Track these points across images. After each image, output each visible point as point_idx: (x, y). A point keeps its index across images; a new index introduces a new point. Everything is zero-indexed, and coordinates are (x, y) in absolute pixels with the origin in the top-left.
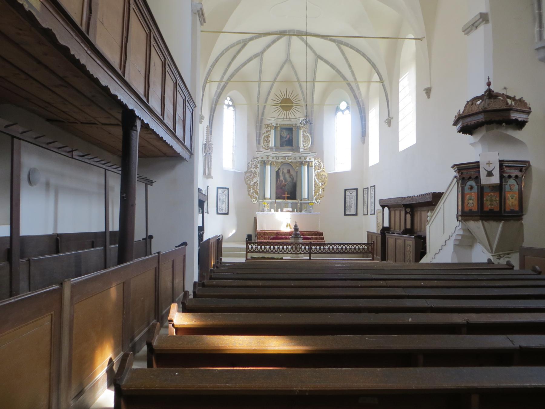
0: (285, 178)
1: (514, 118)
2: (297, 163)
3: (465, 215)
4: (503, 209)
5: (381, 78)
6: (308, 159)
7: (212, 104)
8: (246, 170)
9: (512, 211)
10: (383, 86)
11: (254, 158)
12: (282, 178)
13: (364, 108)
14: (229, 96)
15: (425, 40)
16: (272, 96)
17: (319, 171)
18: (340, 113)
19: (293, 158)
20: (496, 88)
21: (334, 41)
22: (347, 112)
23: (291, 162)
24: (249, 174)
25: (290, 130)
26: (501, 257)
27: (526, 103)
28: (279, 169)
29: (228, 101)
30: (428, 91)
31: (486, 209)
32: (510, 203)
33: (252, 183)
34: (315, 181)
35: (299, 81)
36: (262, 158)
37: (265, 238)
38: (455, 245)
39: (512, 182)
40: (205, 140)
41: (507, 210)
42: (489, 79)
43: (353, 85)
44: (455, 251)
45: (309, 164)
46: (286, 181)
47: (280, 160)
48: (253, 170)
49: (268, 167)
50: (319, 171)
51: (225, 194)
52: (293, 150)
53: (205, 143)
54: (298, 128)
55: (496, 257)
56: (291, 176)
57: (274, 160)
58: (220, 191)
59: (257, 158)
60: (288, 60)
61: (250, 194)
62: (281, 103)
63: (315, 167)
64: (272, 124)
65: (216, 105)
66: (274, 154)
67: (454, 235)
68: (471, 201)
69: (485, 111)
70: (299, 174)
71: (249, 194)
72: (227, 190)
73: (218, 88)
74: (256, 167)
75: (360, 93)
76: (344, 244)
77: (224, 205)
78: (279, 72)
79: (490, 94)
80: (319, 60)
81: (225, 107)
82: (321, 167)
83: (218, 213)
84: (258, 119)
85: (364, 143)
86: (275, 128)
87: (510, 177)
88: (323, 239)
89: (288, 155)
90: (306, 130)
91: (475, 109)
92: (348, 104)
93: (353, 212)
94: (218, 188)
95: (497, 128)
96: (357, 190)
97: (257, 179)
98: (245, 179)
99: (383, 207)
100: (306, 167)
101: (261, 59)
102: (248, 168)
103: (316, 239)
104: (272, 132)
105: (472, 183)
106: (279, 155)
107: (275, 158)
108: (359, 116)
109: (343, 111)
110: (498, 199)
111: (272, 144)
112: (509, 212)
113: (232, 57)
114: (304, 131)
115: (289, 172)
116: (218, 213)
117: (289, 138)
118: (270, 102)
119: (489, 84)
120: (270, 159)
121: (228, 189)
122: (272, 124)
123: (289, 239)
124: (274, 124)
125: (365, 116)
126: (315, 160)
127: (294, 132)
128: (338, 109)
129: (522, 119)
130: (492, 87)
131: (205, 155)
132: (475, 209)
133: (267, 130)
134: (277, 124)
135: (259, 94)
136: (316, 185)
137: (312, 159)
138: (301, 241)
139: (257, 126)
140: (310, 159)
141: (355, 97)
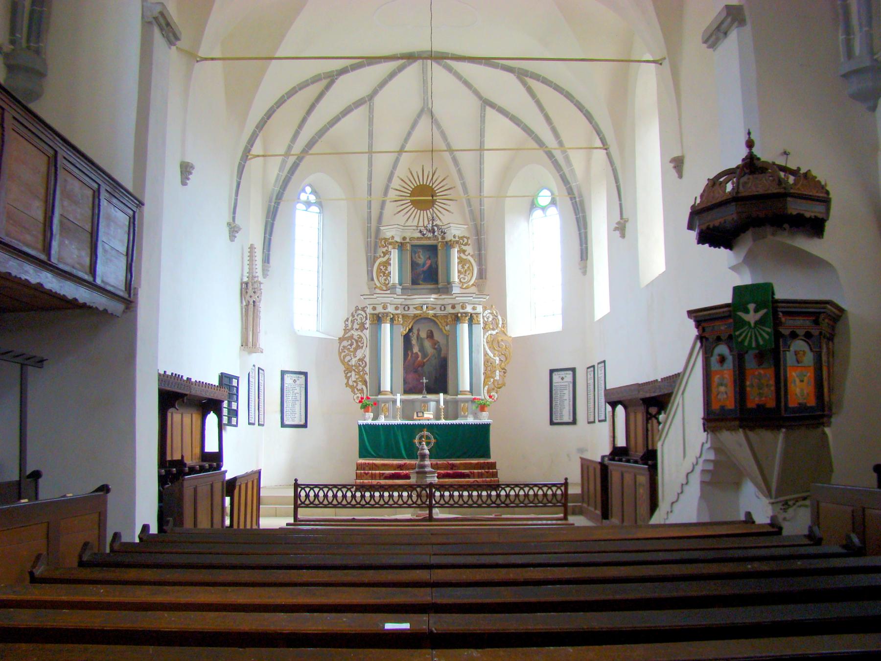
0: (423, 348)
1: (794, 213)
2: (446, 316)
3: (714, 420)
4: (783, 404)
5: (603, 140)
6: (469, 309)
7: (270, 201)
8: (341, 334)
9: (802, 408)
10: (608, 155)
11: (357, 309)
12: (416, 350)
13: (582, 203)
14: (310, 185)
15: (666, 63)
16: (396, 183)
17: (494, 332)
18: (537, 213)
19: (438, 307)
20: (765, 154)
21: (510, 70)
22: (553, 210)
23: (435, 315)
24: (348, 343)
25: (432, 250)
26: (789, 506)
27: (819, 182)
28: (410, 330)
29: (307, 195)
30: (678, 164)
31: (751, 405)
32: (798, 390)
33: (353, 362)
34: (486, 354)
35: (450, 150)
36: (374, 308)
37: (373, 477)
38: (703, 483)
39: (799, 345)
40: (246, 274)
41: (791, 405)
42: (749, 134)
43: (558, 155)
44: (703, 496)
45: (472, 319)
46: (425, 355)
47: (412, 312)
48: (356, 334)
49: (386, 327)
50: (494, 332)
51: (300, 385)
52: (438, 291)
53: (245, 279)
54: (448, 245)
55: (780, 506)
56: (435, 344)
57: (399, 312)
58: (288, 379)
59: (363, 309)
60: (426, 110)
61: (351, 383)
62: (413, 194)
63: (485, 323)
64: (393, 237)
65: (279, 204)
66: (400, 300)
67: (701, 461)
68: (722, 389)
69: (736, 199)
70: (452, 338)
71: (347, 384)
72: (303, 377)
73: (281, 169)
74: (362, 327)
75: (572, 171)
76: (531, 486)
77: (297, 407)
78: (409, 134)
79: (752, 165)
80: (488, 109)
81: (300, 206)
82: (497, 324)
83: (283, 425)
84: (369, 229)
85: (584, 273)
86: (401, 246)
87: (794, 336)
88: (495, 475)
89: (426, 301)
90: (464, 248)
91: (719, 197)
92: (552, 194)
93: (567, 418)
94: (283, 373)
95: (773, 234)
96: (573, 370)
97: (365, 352)
98: (340, 353)
99: (614, 405)
100: (465, 326)
101: (371, 110)
102: (346, 330)
103: (480, 475)
104: (395, 255)
105: (722, 349)
106: (408, 302)
107: (401, 308)
108: (573, 217)
109: (544, 209)
110: (772, 382)
111: (395, 278)
112: (794, 410)
113: (307, 108)
114: (462, 251)
115: (431, 335)
116: (283, 425)
117: (431, 266)
118: (392, 194)
119: (750, 144)
120: (390, 309)
121: (305, 374)
122: (393, 237)
123: (407, 477)
124: (398, 239)
125: (584, 218)
126: (485, 309)
127: (440, 253)
128: (533, 206)
129: (813, 215)
130: (756, 151)
131: (247, 306)
132: (730, 405)
133: (384, 250)
134: (404, 238)
135: (370, 178)
136: (487, 361)
137: (479, 309)
138: (435, 480)
139: (368, 245)
140: (474, 308)
141: (563, 180)
